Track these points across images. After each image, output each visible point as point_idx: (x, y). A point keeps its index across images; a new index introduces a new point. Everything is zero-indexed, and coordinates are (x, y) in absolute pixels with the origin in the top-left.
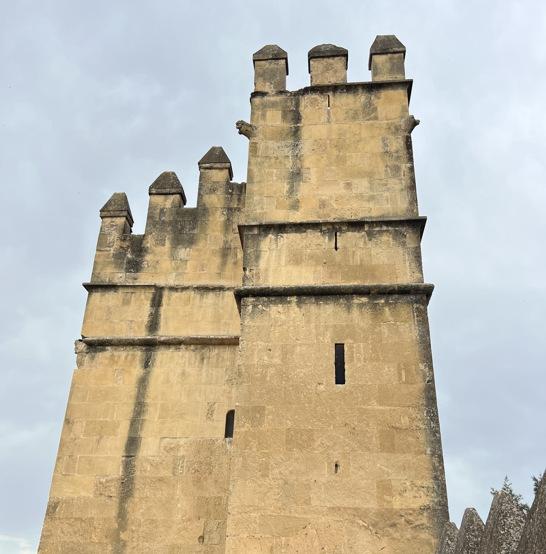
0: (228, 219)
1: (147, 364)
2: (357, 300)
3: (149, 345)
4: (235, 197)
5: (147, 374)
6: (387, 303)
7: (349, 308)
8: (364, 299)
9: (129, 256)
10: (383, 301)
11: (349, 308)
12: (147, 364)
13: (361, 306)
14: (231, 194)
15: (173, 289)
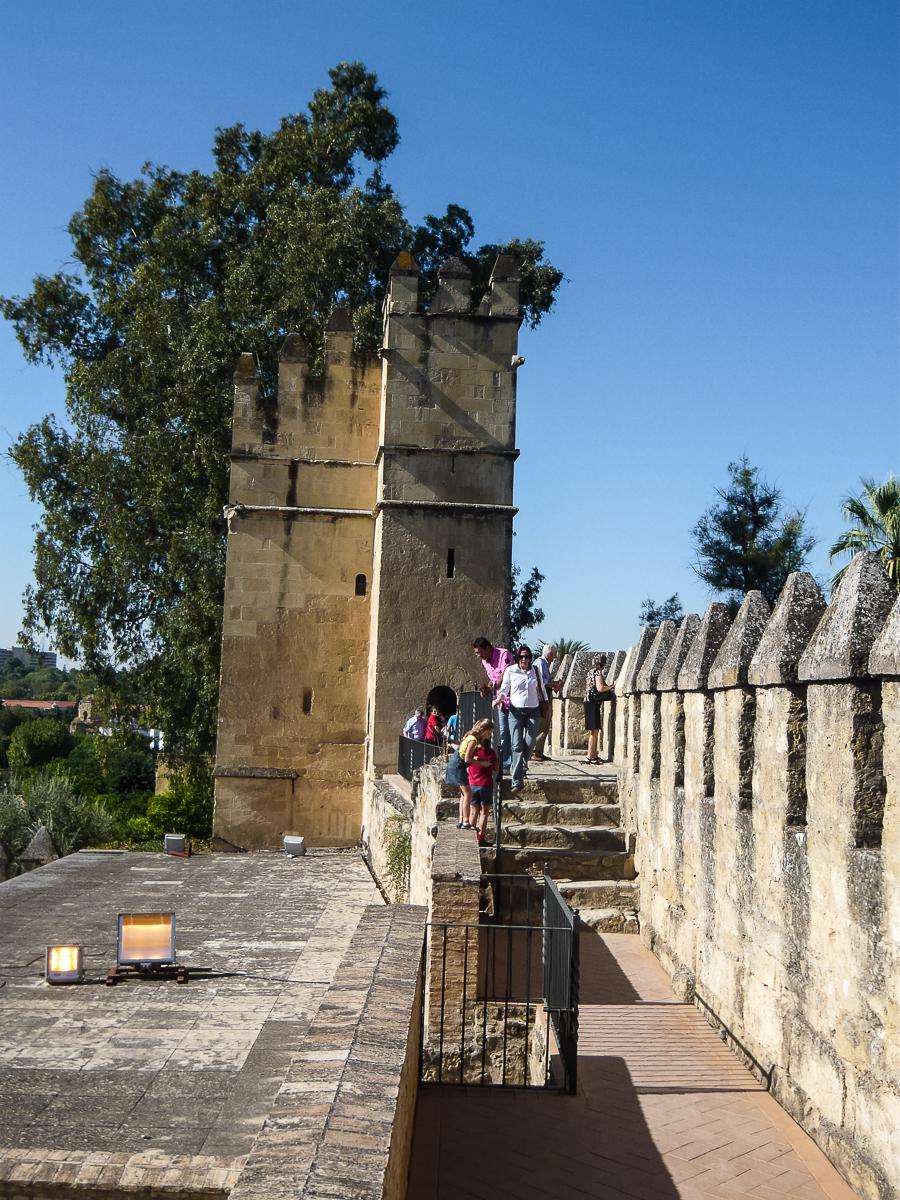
0: (354, 393)
1: (288, 531)
2: (465, 517)
3: (291, 517)
4: (360, 370)
5: (290, 540)
6: (486, 520)
7: (459, 521)
8: (471, 516)
9: (264, 426)
10: (483, 518)
11: (459, 521)
12: (288, 531)
13: (468, 520)
14: (355, 366)
15: (305, 462)
